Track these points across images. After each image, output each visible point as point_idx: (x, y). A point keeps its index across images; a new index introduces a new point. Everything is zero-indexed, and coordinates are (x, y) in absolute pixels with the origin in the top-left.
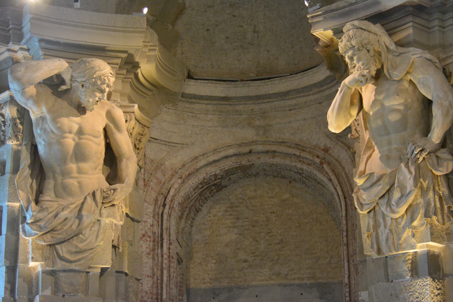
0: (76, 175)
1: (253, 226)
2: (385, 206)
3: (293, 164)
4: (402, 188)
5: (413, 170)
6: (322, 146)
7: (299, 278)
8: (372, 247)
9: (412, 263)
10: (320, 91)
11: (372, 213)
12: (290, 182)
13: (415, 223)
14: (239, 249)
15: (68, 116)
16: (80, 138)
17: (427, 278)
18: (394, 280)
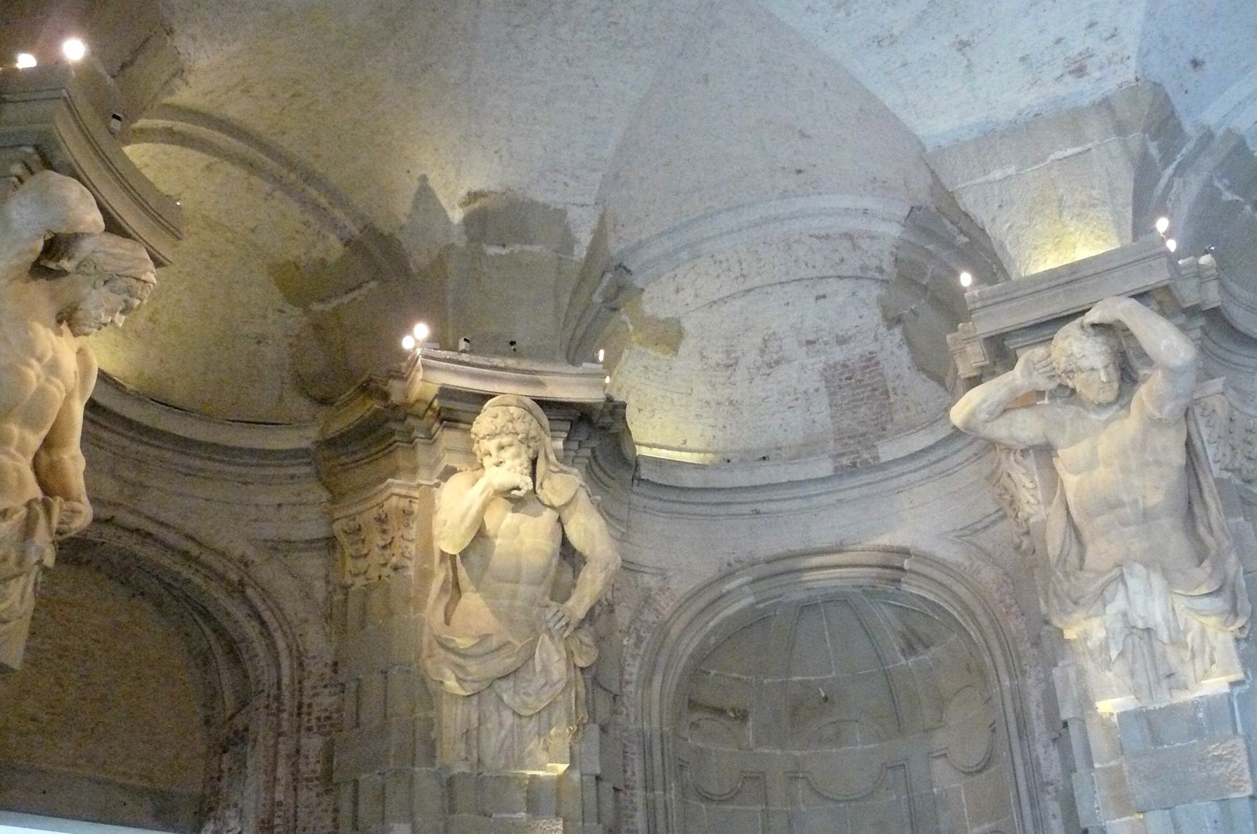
0: (13, 450)
1: (60, 657)
2: (511, 692)
3: (177, 568)
4: (546, 670)
5: (562, 648)
6: (237, 553)
7: (124, 774)
8: (469, 751)
9: (528, 791)
10: (258, 465)
11: (475, 700)
12: (134, 595)
13: (553, 732)
14: (28, 692)
15: (46, 326)
16: (47, 380)
17: (558, 820)
18: (494, 816)
